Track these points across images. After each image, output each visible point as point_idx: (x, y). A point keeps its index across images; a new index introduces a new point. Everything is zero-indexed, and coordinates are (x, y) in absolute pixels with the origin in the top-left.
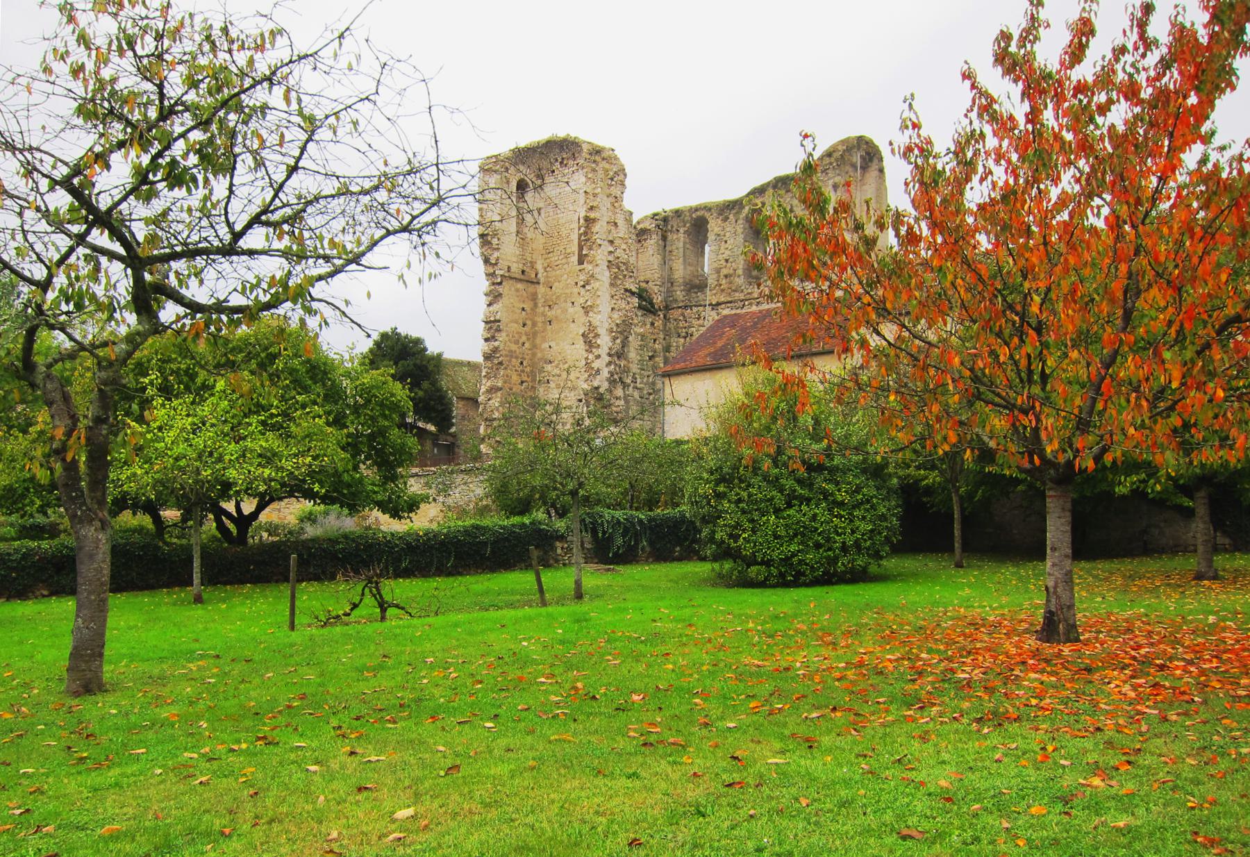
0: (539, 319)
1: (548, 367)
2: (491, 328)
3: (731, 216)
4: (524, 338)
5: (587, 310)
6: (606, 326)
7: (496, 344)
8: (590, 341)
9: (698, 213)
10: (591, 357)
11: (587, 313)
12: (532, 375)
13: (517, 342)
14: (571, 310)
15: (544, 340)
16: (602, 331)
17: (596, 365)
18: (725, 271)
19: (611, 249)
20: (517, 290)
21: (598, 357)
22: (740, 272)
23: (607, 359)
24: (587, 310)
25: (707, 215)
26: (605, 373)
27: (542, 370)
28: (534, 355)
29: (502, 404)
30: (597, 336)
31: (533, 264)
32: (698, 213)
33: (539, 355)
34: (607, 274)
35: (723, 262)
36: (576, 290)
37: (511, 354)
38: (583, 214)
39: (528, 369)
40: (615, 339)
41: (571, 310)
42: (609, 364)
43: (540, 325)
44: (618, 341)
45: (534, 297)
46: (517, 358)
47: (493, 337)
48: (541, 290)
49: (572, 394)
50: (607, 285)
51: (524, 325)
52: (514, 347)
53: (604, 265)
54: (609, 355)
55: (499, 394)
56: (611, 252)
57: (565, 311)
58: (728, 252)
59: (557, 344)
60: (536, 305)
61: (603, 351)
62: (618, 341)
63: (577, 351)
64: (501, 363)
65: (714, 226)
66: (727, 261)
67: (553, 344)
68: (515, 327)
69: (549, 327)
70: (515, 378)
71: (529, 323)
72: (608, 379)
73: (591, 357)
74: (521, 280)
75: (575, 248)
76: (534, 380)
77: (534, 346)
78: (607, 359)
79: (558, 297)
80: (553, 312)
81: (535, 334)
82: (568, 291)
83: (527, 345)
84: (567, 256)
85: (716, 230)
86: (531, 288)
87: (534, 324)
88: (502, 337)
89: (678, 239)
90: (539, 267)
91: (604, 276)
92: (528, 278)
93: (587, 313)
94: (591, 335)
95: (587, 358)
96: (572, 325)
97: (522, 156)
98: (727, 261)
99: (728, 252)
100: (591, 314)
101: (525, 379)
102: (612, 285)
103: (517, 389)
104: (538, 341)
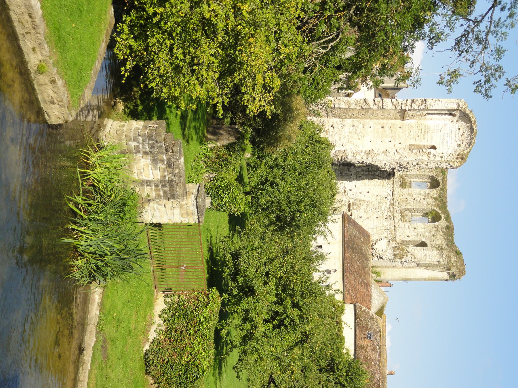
1: (360, 127)
22: (408, 207)
28: (367, 118)
36: (396, 143)
49: (346, 141)
58: (419, 199)
60: (392, 119)
65: (434, 192)
66: (414, 199)
69: (380, 126)
73: (363, 154)
75: (418, 143)
76: (354, 118)
93: (384, 152)
95: (362, 152)
98: (414, 199)
99: (419, 199)
100: (383, 154)
101: (355, 115)
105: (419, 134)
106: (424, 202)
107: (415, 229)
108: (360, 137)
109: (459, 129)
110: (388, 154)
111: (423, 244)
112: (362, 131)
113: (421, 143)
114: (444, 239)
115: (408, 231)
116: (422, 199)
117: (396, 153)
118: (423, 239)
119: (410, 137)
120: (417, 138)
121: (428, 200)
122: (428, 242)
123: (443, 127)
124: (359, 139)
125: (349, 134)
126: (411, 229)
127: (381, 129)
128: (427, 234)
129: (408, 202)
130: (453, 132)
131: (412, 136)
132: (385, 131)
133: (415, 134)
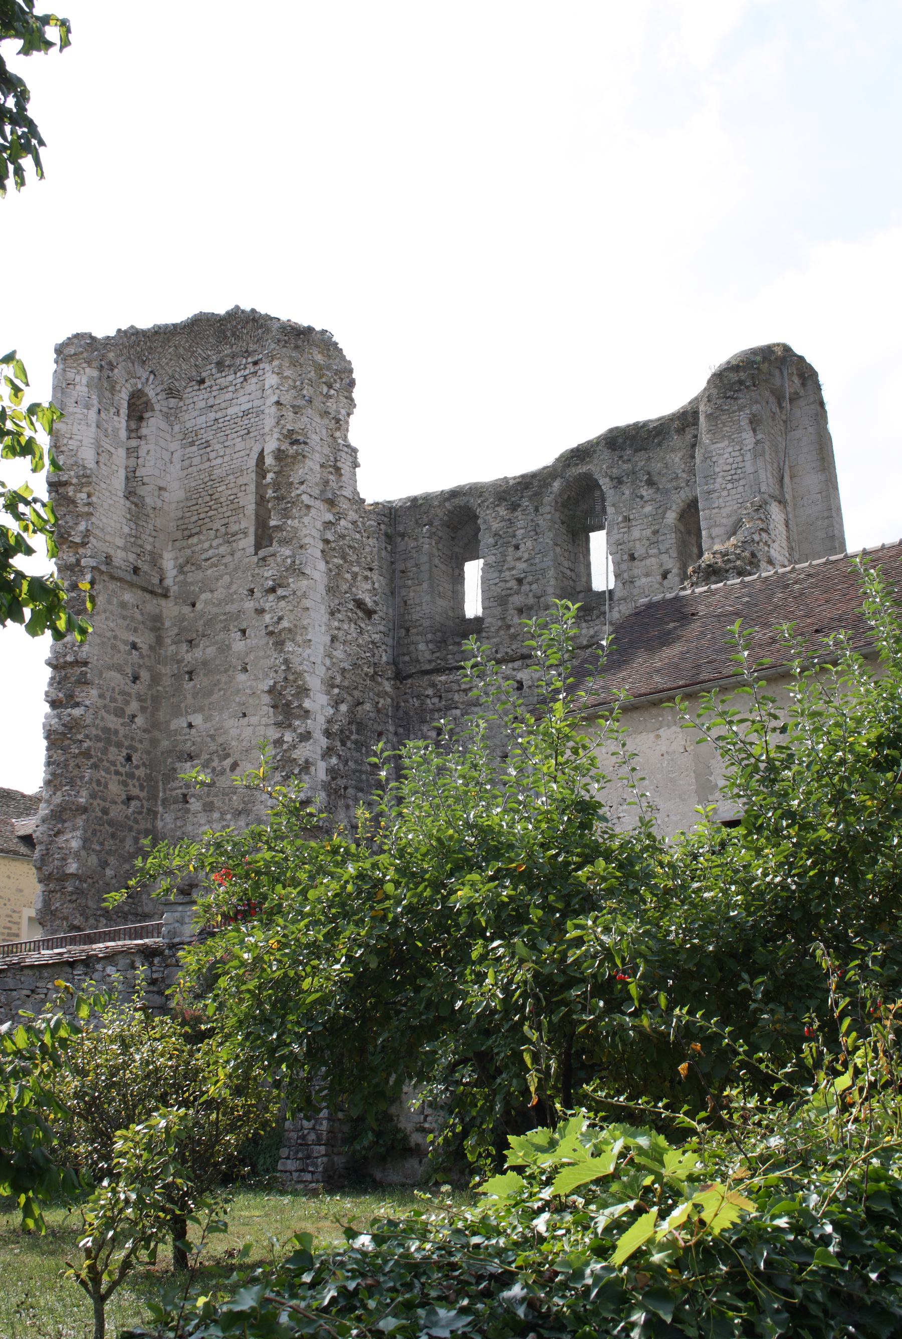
0: (166, 670)
2: (66, 678)
3: (525, 503)
4: (134, 706)
5: (278, 638)
6: (321, 671)
7: (77, 712)
8: (286, 706)
9: (456, 501)
10: (288, 737)
11: (280, 645)
12: (150, 784)
13: (119, 713)
14: (239, 646)
15: (177, 712)
16: (314, 682)
17: (302, 752)
18: (517, 600)
19: (329, 517)
20: (123, 605)
21: (306, 736)
23: (324, 742)
24: (278, 638)
25: (474, 502)
26: (320, 771)
27: (171, 775)
28: (154, 742)
29: (86, 842)
30: (303, 691)
31: (155, 560)
32: (456, 501)
33: (165, 744)
34: (322, 566)
35: (513, 584)
37: (108, 737)
38: (271, 445)
39: (141, 772)
40: (336, 703)
41: (239, 646)
42: (328, 752)
43: (167, 681)
44: (343, 708)
45: (156, 624)
46: (119, 745)
47: (70, 696)
48: (170, 609)
50: (321, 589)
51: (136, 678)
52: (113, 722)
53: (315, 550)
54: (328, 733)
55: (80, 821)
56: (328, 525)
57: (224, 649)
58: (522, 566)
59: (207, 719)
60: (159, 640)
61: (317, 725)
62: (343, 708)
63: (250, 730)
64: (87, 754)
65: (492, 520)
67: (197, 719)
68: (115, 678)
70: (114, 788)
71: (145, 675)
72: (326, 786)
74: (132, 585)
75: (248, 523)
76: (153, 797)
77: (154, 724)
78: (324, 742)
79: (209, 623)
80: (198, 653)
81: (156, 700)
82: (232, 608)
83: (140, 721)
84: (229, 538)
85: (495, 526)
86: (152, 605)
87: (156, 679)
88: (90, 696)
89: (419, 549)
90: (169, 563)
91: (318, 571)
92: (143, 580)
93: (280, 645)
94: (289, 692)
95: (279, 742)
96: (242, 677)
97: (139, 345)
98: (520, 581)
100: (289, 647)
101: (135, 791)
102: (330, 590)
103: (117, 812)
104: (161, 715)
105: (217, 525)
106: (529, 544)
107: (632, 558)
108: (228, 762)
109: (202, 381)
110: (285, 624)
111: (690, 514)
112: (205, 756)
113: (251, 509)
114: (660, 444)
115: (644, 580)
116: (519, 554)
117: (280, 592)
118: (671, 517)
119: (228, 559)
120: (234, 528)
121: (520, 533)
122: (678, 500)
123: (192, 444)
124: (234, 766)
125: (216, 815)
126: (636, 572)
127: (201, 681)
128: (648, 509)
129: (531, 601)
130: (211, 402)
131: (223, 550)
132: (205, 663)
133: (215, 543)
